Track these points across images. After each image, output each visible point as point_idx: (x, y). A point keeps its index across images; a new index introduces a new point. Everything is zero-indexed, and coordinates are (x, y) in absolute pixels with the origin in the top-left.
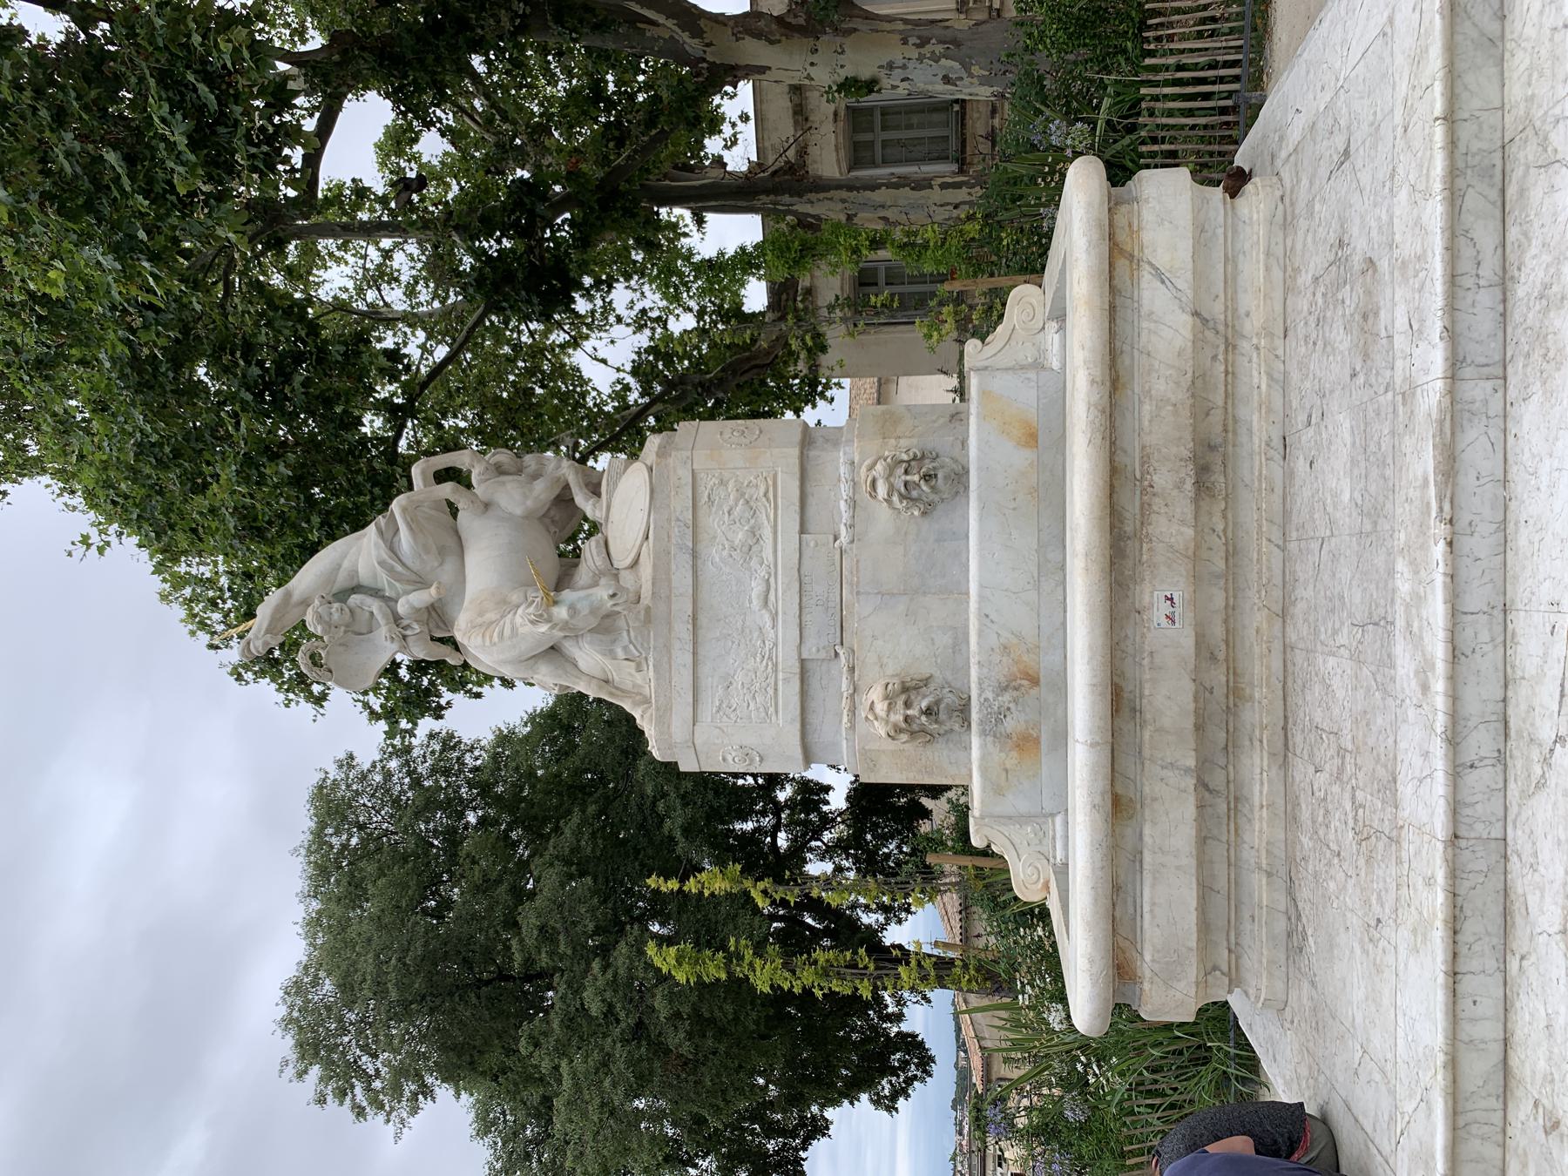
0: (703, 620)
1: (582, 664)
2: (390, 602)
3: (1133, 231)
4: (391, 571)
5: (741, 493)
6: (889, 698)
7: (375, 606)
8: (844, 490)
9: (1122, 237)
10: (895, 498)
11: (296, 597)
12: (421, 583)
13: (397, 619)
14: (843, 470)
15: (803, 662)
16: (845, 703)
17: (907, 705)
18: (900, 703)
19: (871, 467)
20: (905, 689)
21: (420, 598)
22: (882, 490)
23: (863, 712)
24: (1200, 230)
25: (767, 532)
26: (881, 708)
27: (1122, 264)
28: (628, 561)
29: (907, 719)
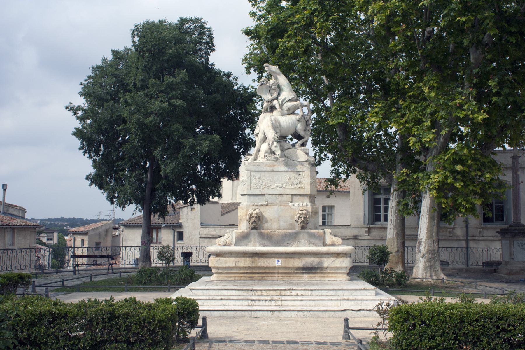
0: (273, 173)
1: (263, 145)
2: (277, 98)
3: (341, 257)
4: (284, 100)
5: (301, 182)
6: (257, 214)
7: (275, 95)
8: (301, 204)
9: (341, 255)
10: (298, 215)
11: (278, 76)
12: (281, 105)
13: (273, 100)
14: (305, 204)
15: (264, 195)
16: (256, 204)
17: (256, 217)
18: (256, 216)
19: (305, 210)
20: (259, 216)
21: (277, 106)
22: (300, 212)
23: (254, 207)
24: (341, 268)
25: (292, 187)
26: (255, 212)
27: (336, 255)
28: (286, 155)
29: (253, 217)
